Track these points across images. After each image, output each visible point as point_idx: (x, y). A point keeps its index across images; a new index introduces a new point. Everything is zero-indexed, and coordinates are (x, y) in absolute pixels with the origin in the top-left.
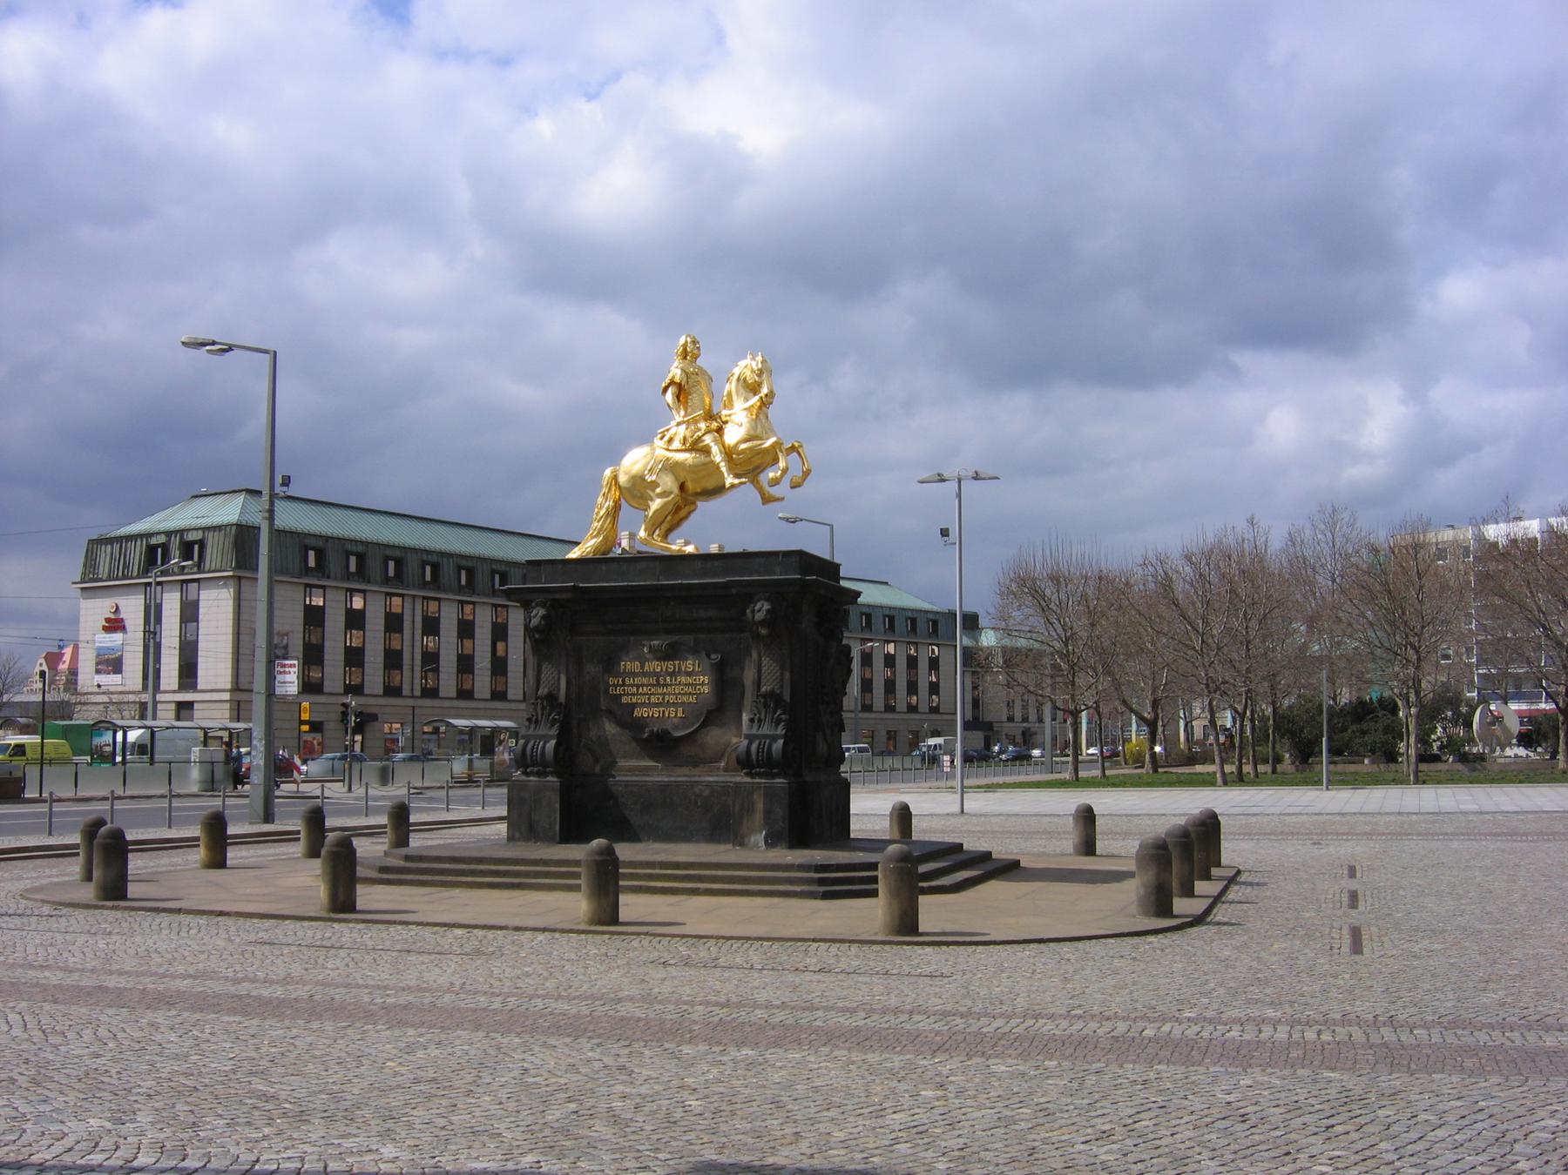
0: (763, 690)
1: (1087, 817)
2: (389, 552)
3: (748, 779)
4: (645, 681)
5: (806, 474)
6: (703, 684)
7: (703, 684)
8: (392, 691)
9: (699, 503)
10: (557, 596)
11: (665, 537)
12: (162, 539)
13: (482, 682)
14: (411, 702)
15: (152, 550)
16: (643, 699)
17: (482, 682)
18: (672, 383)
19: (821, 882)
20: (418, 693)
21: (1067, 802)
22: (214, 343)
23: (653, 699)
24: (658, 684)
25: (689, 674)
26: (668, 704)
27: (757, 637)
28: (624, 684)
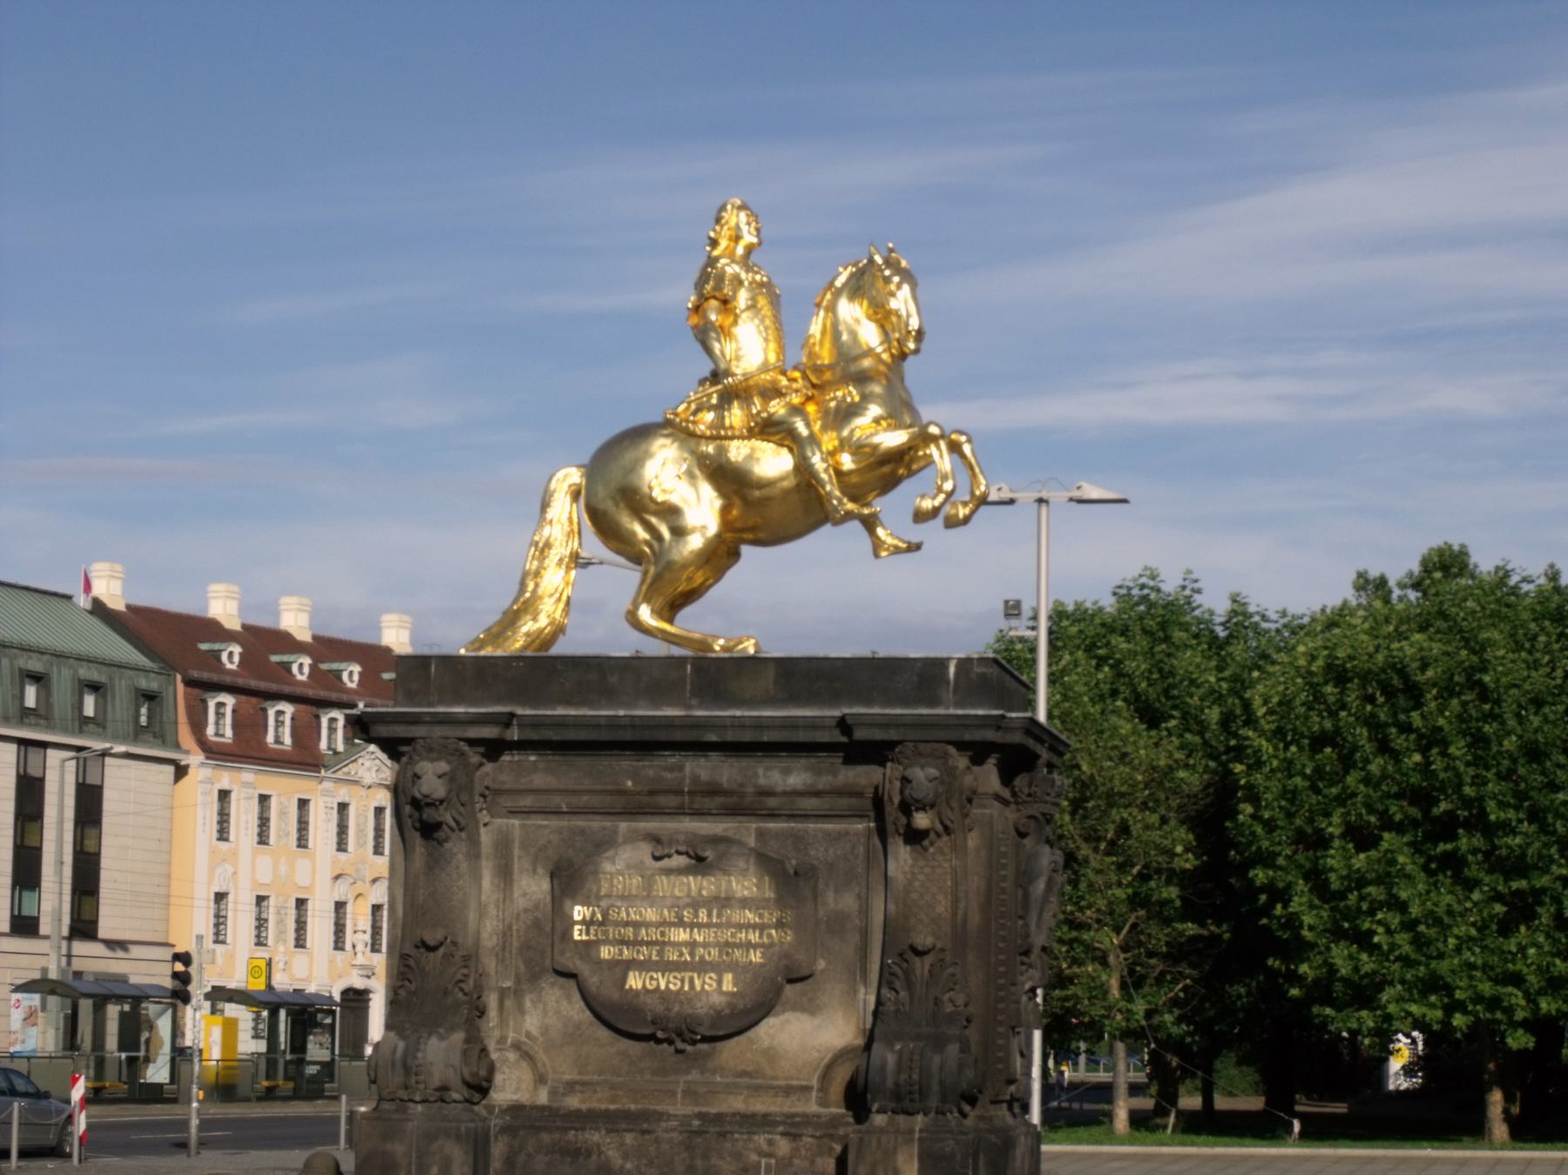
4: (651, 915)
9: (746, 550)
10: (473, 732)
16: (643, 953)
23: (673, 956)
24: (680, 923)
25: (745, 903)
26: (702, 967)
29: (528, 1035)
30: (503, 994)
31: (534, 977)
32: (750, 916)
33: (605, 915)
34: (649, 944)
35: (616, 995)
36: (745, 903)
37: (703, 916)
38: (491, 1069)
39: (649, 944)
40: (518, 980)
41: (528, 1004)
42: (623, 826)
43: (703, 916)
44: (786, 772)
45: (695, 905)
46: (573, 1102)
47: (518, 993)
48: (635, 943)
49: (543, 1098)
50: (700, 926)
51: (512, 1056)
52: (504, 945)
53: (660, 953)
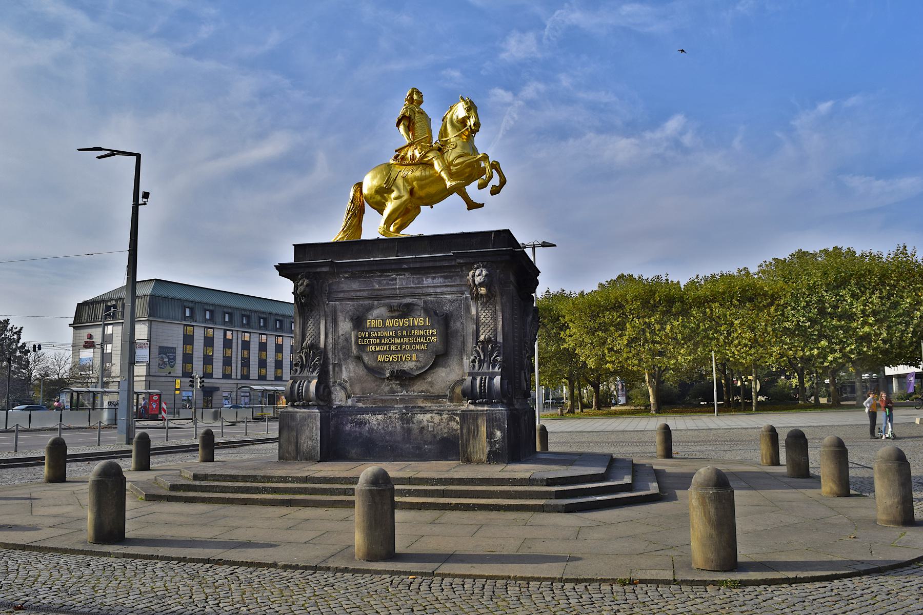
0: (482, 338)
1: (667, 431)
2: (225, 310)
3: (472, 407)
4: (386, 334)
5: (503, 182)
6: (432, 335)
7: (432, 335)
8: (227, 376)
11: (398, 230)
12: (113, 303)
13: (271, 372)
14: (236, 382)
15: (108, 308)
17: (271, 372)
18: (404, 117)
19: (559, 495)
20: (239, 377)
21: (652, 424)
22: (100, 149)
23: (393, 347)
24: (396, 336)
25: (420, 328)
27: (476, 297)
28: (369, 337)
29: (344, 380)
30: (334, 365)
31: (345, 359)
32: (422, 333)
33: (369, 335)
34: (386, 344)
35: (374, 364)
36: (420, 328)
37: (404, 333)
38: (330, 393)
39: (386, 344)
40: (339, 359)
41: (344, 369)
42: (376, 302)
43: (404, 333)
44: (433, 278)
45: (402, 328)
46: (360, 405)
47: (340, 366)
48: (380, 344)
49: (350, 403)
50: (402, 337)
51: (338, 388)
52: (334, 348)
53: (390, 348)
